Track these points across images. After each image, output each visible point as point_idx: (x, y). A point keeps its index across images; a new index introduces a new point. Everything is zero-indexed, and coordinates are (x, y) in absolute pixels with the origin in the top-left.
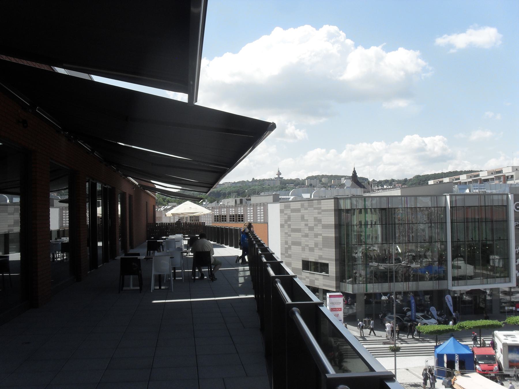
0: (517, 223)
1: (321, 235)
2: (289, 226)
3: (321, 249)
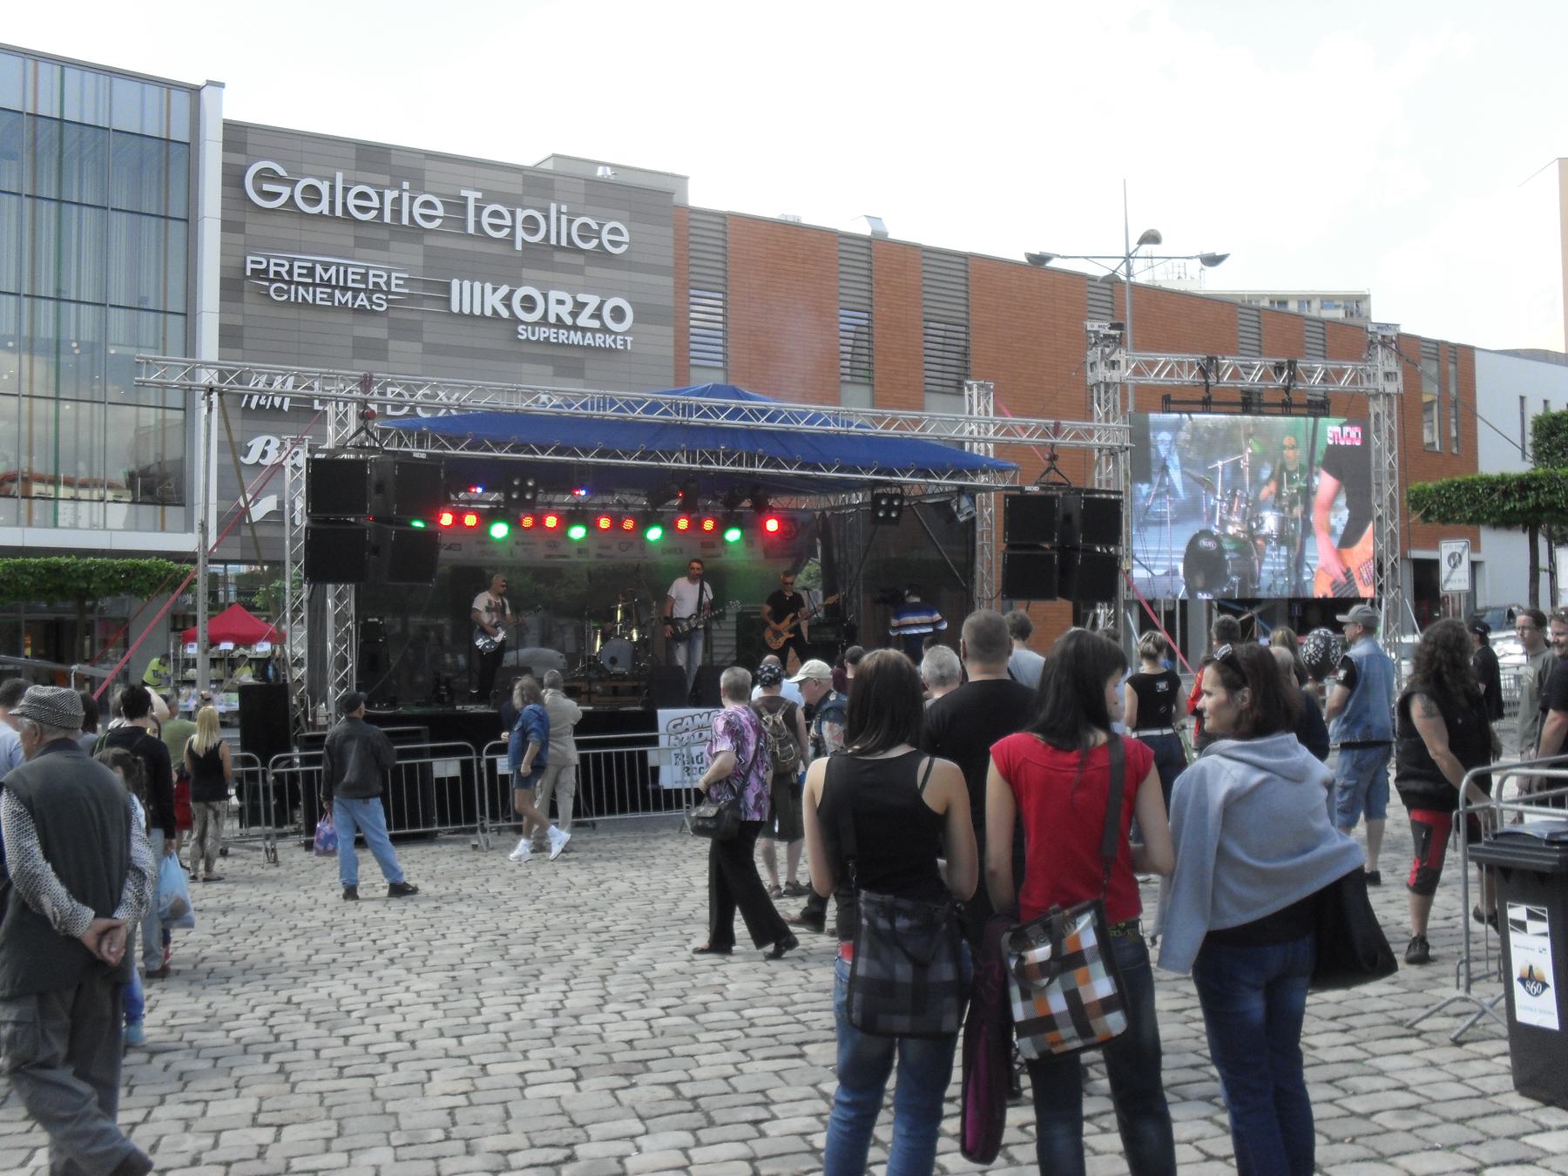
0: (260, 263)
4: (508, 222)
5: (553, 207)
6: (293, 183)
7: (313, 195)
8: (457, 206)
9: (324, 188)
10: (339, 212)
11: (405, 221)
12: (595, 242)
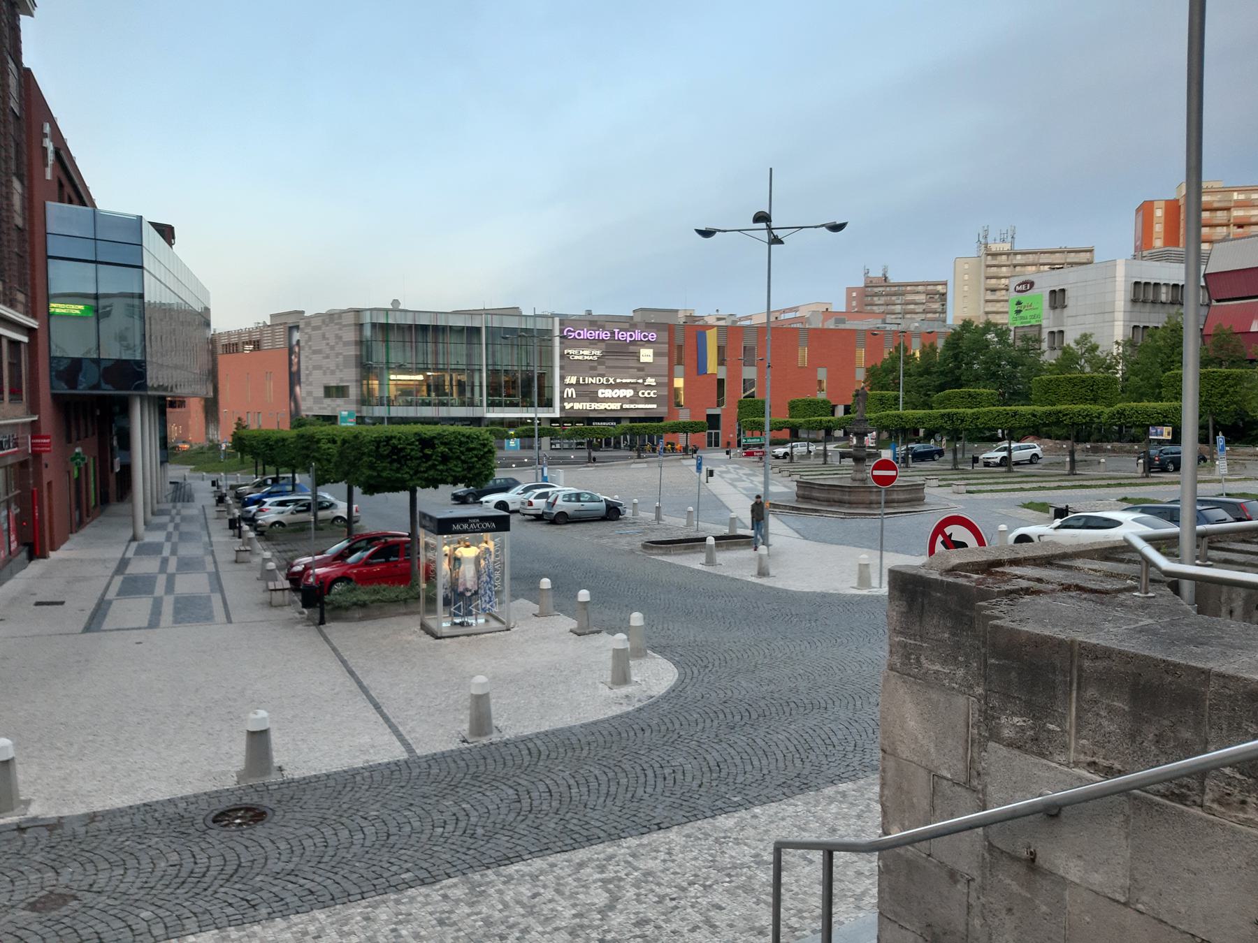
1: (341, 354)
2: (310, 347)
3: (341, 371)
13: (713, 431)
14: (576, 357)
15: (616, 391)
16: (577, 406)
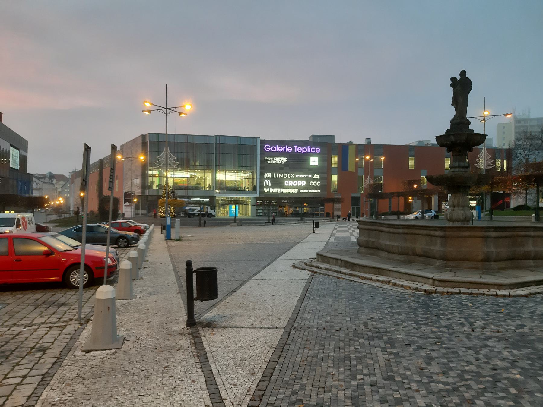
4: (301, 149)
5: (308, 147)
6: (271, 147)
7: (273, 149)
8: (294, 148)
9: (275, 147)
10: (277, 151)
11: (286, 151)
12: (314, 151)
13: (356, 207)
14: (272, 162)
15: (296, 182)
16: (272, 190)
